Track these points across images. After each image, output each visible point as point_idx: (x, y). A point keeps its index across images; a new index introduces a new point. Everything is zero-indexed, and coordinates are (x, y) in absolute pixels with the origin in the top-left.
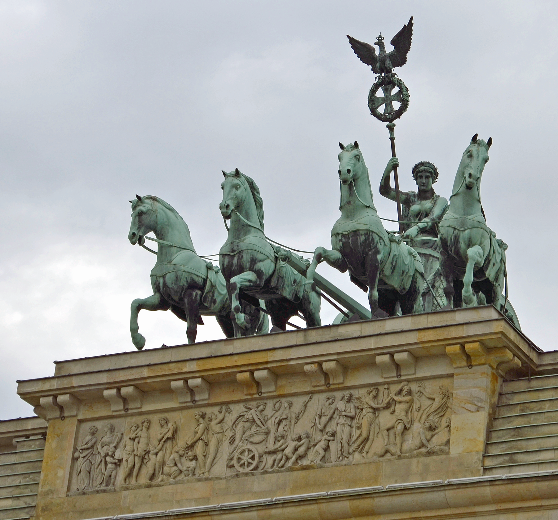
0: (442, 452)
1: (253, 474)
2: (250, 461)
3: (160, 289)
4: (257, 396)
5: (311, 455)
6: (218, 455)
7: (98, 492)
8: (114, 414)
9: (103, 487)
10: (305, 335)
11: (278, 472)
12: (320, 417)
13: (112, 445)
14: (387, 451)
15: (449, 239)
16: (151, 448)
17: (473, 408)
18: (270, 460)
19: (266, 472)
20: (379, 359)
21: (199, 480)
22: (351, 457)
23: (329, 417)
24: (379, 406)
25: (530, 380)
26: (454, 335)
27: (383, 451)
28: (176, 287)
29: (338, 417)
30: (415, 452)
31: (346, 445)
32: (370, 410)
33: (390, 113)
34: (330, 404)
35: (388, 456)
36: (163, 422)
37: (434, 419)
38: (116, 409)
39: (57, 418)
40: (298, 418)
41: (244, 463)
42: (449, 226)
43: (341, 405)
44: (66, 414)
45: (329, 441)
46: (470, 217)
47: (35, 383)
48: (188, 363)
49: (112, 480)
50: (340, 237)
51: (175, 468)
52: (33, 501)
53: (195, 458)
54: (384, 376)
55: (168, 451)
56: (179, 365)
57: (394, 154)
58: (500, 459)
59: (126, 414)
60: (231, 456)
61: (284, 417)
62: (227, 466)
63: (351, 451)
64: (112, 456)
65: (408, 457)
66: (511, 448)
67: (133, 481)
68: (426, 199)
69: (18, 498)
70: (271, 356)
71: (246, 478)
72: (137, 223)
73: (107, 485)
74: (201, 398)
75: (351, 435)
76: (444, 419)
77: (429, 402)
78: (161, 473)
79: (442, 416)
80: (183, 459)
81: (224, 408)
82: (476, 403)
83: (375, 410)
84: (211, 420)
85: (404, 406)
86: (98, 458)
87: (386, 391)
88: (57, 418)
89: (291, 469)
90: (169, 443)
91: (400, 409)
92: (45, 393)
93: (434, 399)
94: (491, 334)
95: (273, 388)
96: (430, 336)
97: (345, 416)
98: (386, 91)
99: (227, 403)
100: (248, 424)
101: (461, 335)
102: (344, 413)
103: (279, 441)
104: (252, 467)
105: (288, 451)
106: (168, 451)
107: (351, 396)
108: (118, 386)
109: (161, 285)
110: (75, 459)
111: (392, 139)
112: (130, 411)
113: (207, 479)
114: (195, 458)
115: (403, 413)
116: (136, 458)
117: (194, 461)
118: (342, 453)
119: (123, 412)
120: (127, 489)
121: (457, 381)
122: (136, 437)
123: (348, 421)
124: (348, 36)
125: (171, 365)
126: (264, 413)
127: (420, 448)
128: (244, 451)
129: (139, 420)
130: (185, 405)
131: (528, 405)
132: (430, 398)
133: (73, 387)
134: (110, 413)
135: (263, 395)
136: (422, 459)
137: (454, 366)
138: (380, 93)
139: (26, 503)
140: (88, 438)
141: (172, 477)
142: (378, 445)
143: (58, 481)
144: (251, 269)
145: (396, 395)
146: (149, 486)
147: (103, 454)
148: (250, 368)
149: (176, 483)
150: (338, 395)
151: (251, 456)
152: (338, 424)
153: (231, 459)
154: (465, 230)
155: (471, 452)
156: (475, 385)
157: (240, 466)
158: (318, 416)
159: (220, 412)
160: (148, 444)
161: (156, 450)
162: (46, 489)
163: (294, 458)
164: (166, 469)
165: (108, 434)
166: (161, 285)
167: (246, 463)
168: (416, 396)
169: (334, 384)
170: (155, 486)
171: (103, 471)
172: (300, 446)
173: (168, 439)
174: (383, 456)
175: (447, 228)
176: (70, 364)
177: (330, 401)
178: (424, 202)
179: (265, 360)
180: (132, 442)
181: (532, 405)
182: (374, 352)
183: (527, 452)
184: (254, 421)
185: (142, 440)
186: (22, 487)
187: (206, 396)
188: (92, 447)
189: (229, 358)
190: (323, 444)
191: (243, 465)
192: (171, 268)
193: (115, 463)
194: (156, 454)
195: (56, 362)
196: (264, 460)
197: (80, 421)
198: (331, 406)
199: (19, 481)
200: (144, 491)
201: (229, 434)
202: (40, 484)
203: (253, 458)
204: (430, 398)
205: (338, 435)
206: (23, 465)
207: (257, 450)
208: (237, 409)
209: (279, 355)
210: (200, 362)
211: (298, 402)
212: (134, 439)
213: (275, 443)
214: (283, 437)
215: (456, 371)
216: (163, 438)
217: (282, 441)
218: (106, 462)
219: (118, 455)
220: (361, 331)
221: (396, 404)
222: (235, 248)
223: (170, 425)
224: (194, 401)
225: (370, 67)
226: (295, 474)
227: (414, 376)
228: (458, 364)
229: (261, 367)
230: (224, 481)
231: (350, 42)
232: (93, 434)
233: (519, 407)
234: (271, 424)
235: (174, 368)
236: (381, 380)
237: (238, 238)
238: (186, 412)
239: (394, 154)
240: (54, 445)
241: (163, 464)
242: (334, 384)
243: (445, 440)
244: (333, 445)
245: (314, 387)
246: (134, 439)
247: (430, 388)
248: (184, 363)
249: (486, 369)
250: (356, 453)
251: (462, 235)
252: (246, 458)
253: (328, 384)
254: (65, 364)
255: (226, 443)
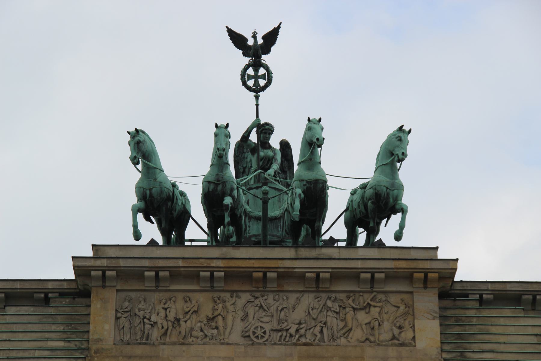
0: (410, 345)
1: (265, 344)
2: (263, 334)
3: (146, 197)
4: (262, 289)
5: (309, 335)
6: (234, 327)
7: (140, 344)
8: (146, 288)
9: (144, 341)
10: (296, 251)
11: (285, 345)
12: (312, 309)
13: (147, 311)
14: (367, 339)
15: (383, 195)
16: (181, 317)
17: (430, 317)
18: (276, 336)
19: (275, 344)
20: (363, 275)
21: (222, 344)
22: (338, 340)
23: (319, 310)
24: (358, 307)
25: (455, 300)
26: (421, 266)
27: (364, 339)
28: (159, 198)
29: (326, 311)
30: (390, 342)
31: (335, 332)
32: (351, 309)
33: (257, 87)
34: (318, 301)
35: (368, 342)
36: (188, 299)
37: (400, 321)
38: (149, 285)
39: (100, 286)
40: (294, 308)
41: (258, 336)
42: (384, 186)
43: (329, 303)
44: (107, 284)
45: (322, 327)
46: (396, 181)
47: (88, 260)
48: (215, 261)
49: (150, 337)
50: (305, 183)
51: (202, 333)
52: (82, 345)
53: (217, 328)
54: (361, 287)
55: (194, 321)
56: (208, 261)
57: (257, 116)
58: (454, 355)
59: (157, 289)
60: (247, 329)
61: (285, 306)
62: (242, 336)
63: (339, 336)
64: (149, 319)
65: (385, 346)
66: (458, 347)
67: (167, 339)
68: (266, 148)
69: (69, 341)
70: (281, 264)
71: (260, 346)
72: (136, 149)
73: (147, 339)
74: (218, 286)
75: (338, 325)
76: (407, 322)
77: (394, 309)
78: (189, 335)
79: (405, 319)
80: (206, 326)
81: (235, 294)
82: (432, 313)
83: (354, 309)
84: (225, 302)
85: (378, 309)
86: (138, 320)
87: (361, 297)
88: (100, 286)
89: (295, 344)
90: (194, 316)
91: (375, 311)
92: (96, 268)
93: (399, 307)
94: (448, 269)
95: (275, 285)
96: (403, 264)
97: (334, 311)
98: (256, 71)
99: (237, 291)
100: (257, 308)
101: (426, 267)
102: (332, 309)
103: (283, 323)
104: (265, 339)
105: (292, 331)
106: (194, 321)
107: (336, 298)
108: (156, 271)
109: (148, 195)
110: (117, 318)
111: (257, 106)
112: (160, 288)
113: (228, 344)
114: (217, 328)
115: (377, 314)
116: (170, 323)
117: (216, 330)
118: (332, 337)
119: (154, 288)
120: (164, 344)
121: (416, 297)
122: (168, 308)
123: (335, 315)
124: (227, 27)
125: (201, 260)
126: (267, 301)
127: (392, 339)
128: (257, 327)
129: (168, 295)
130: (205, 289)
131: (460, 318)
132: (395, 306)
133: (120, 267)
134: (143, 288)
135: (267, 289)
136: (395, 348)
137: (414, 286)
138: (251, 71)
139: (76, 345)
140: (126, 304)
141: (199, 339)
142: (358, 334)
143: (105, 333)
144: (230, 195)
145: (371, 300)
146: (183, 344)
147: (142, 317)
148: (263, 270)
149: (204, 344)
150: (324, 296)
151: (263, 331)
152: (327, 316)
153: (246, 332)
154: (393, 190)
155: (432, 347)
156: (427, 302)
157: (255, 337)
158: (310, 309)
159: (232, 297)
160: (176, 314)
161: (186, 319)
162: (96, 337)
163: (297, 336)
164: (194, 333)
165: (142, 303)
166: (148, 195)
167: (260, 336)
168: (384, 303)
169: (322, 288)
170: (187, 345)
171: (142, 329)
172: (301, 329)
173: (194, 311)
174: (363, 342)
175: (382, 187)
176: (106, 248)
177: (319, 299)
178: (265, 151)
179: (277, 266)
180: (164, 311)
181: (463, 319)
182: (360, 271)
183: (473, 352)
184: (261, 307)
185: (173, 311)
186: (69, 333)
187: (223, 285)
188: (130, 311)
189: (248, 260)
190: (318, 329)
191: (257, 337)
192: (158, 184)
193: (152, 325)
194: (186, 322)
195: (93, 246)
196: (272, 335)
197: (118, 291)
198: (320, 302)
199: (62, 328)
200: (178, 347)
201: (241, 314)
202: (91, 333)
203: (265, 333)
204: (395, 306)
205: (329, 324)
206: (62, 316)
207: (267, 328)
208: (245, 297)
209: (288, 264)
210: (224, 261)
211: (293, 298)
212: (166, 309)
213: (279, 324)
214: (286, 321)
215: (414, 290)
216: (190, 311)
217: (286, 324)
218: (144, 322)
219: (154, 318)
220: (339, 253)
221: (370, 307)
222: (220, 179)
223: (194, 302)
224: (212, 287)
225: (241, 52)
226: (298, 347)
227: (383, 290)
228: (417, 286)
229: (273, 270)
230: (243, 347)
231: (228, 31)
232: (129, 301)
233: (453, 319)
234: (273, 309)
235: (204, 263)
236: (359, 289)
237: (222, 171)
238: (203, 294)
239: (257, 116)
240: (99, 306)
241: (192, 329)
242: (322, 288)
243: (413, 336)
244: (325, 330)
245: (306, 288)
246: (166, 309)
247: (394, 299)
248: (211, 261)
249: (436, 291)
250: (342, 338)
251: (391, 192)
252: (259, 332)
253: (318, 287)
254: (102, 247)
255: (239, 319)
